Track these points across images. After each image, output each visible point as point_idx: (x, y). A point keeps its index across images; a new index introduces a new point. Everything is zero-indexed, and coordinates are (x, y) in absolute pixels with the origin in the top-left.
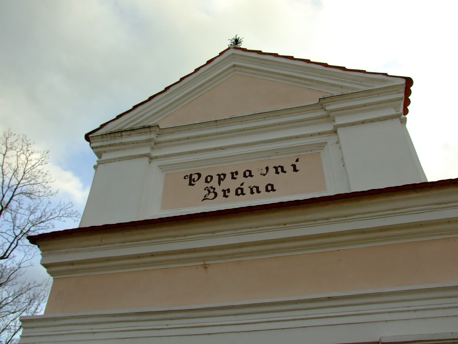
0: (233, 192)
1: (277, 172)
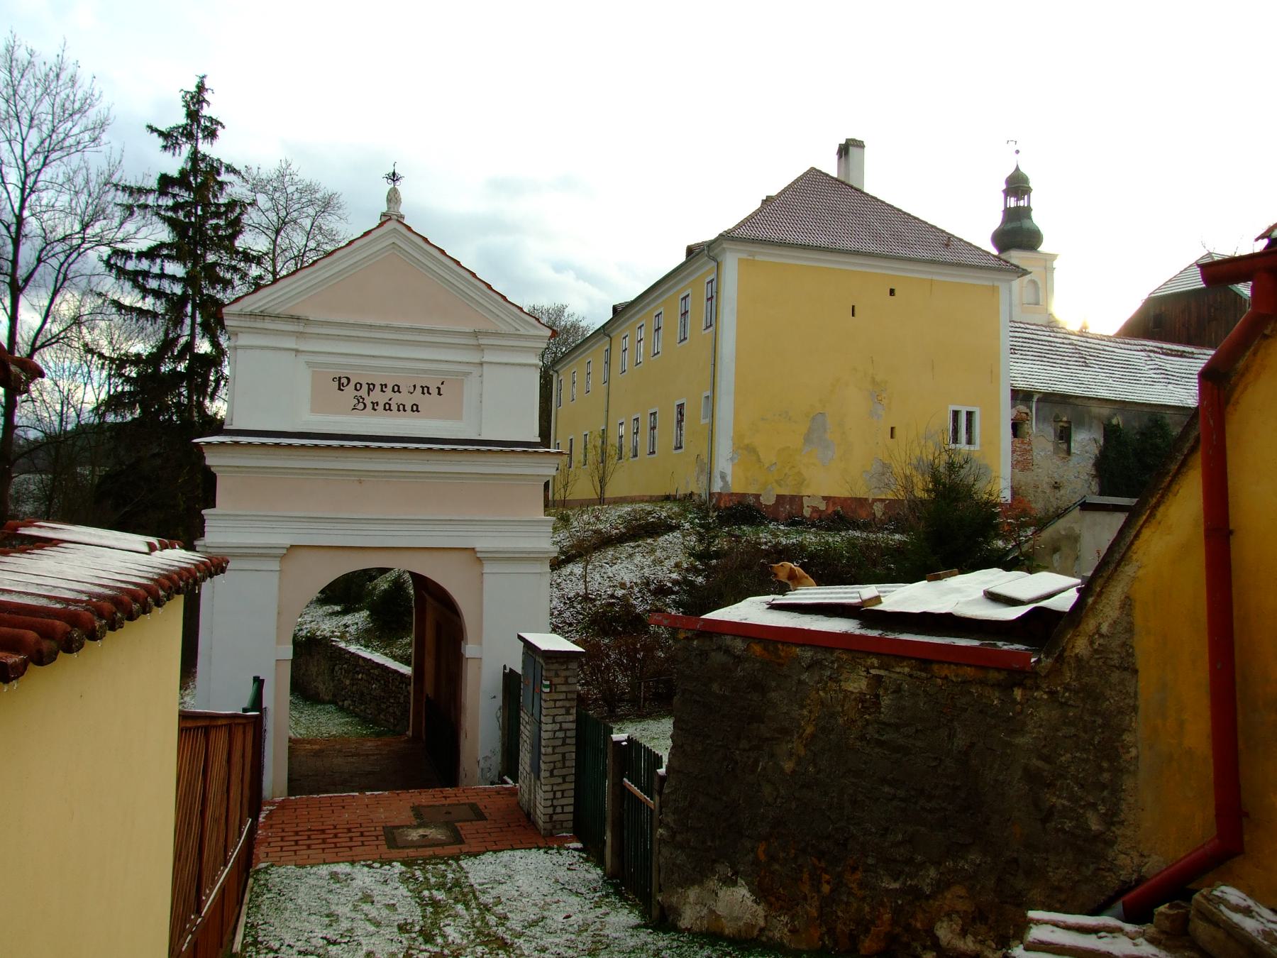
0: (380, 407)
1: (423, 393)
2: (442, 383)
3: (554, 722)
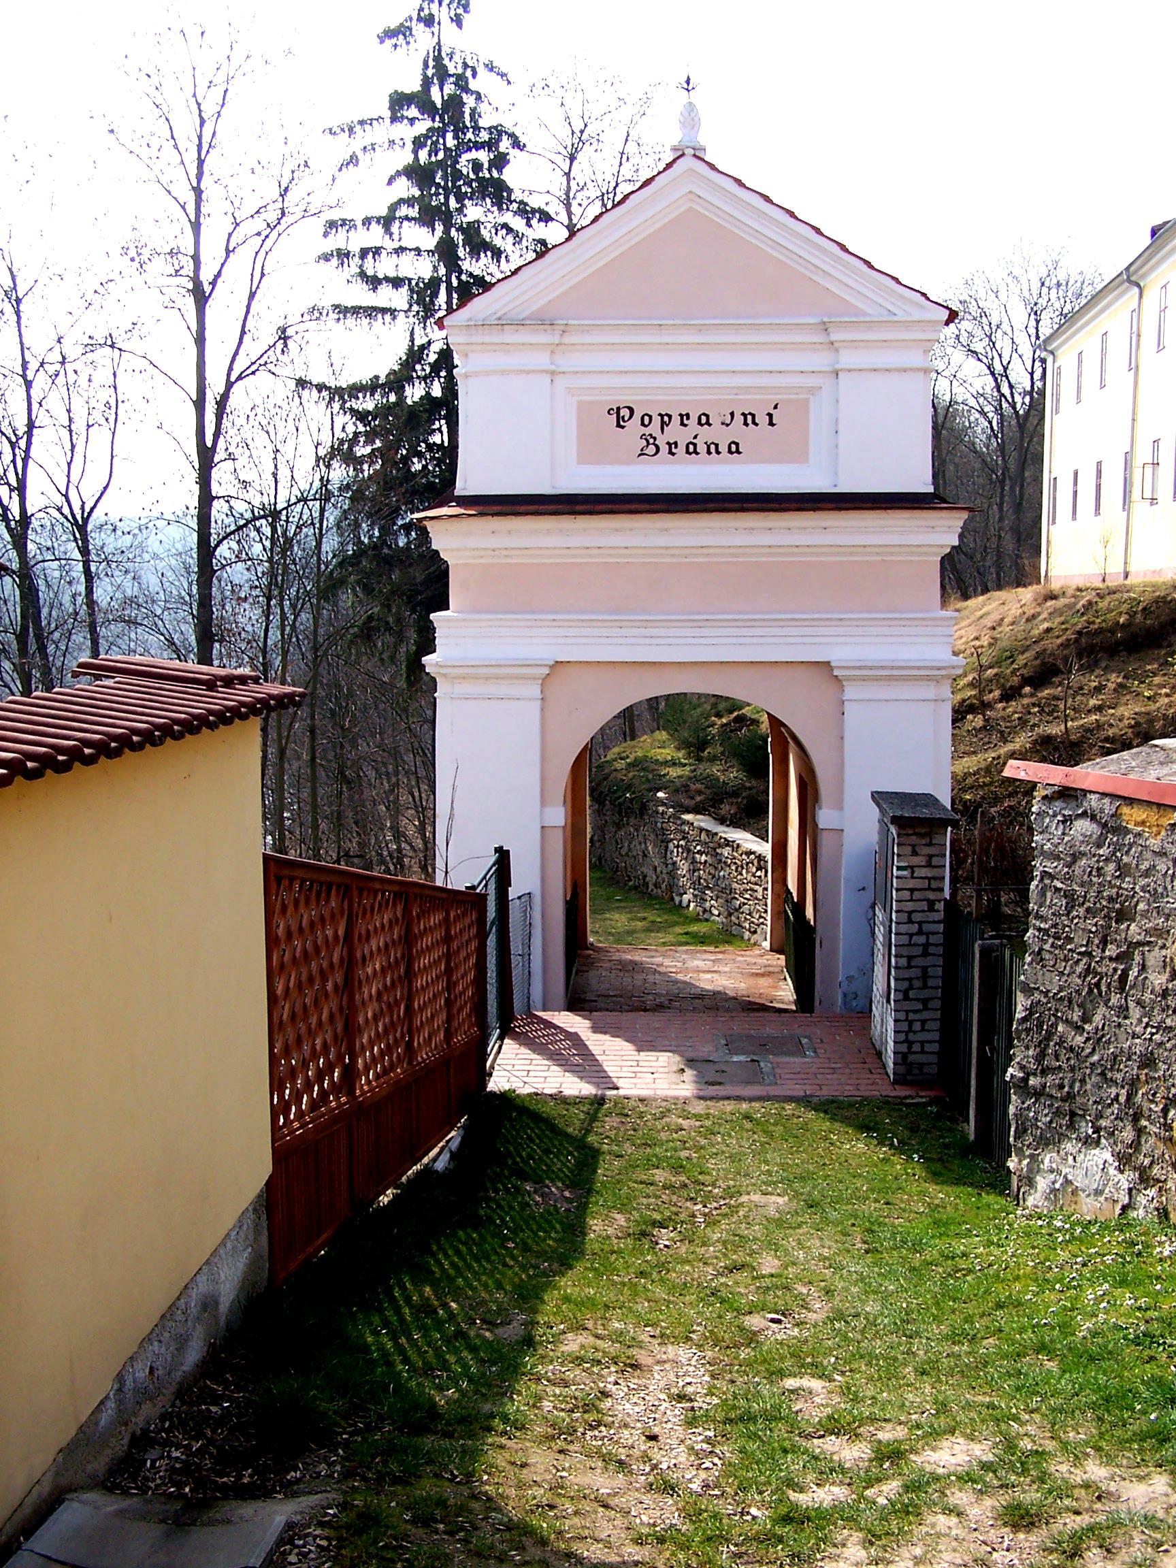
0: (681, 449)
1: (746, 424)
2: (776, 407)
3: (910, 921)
